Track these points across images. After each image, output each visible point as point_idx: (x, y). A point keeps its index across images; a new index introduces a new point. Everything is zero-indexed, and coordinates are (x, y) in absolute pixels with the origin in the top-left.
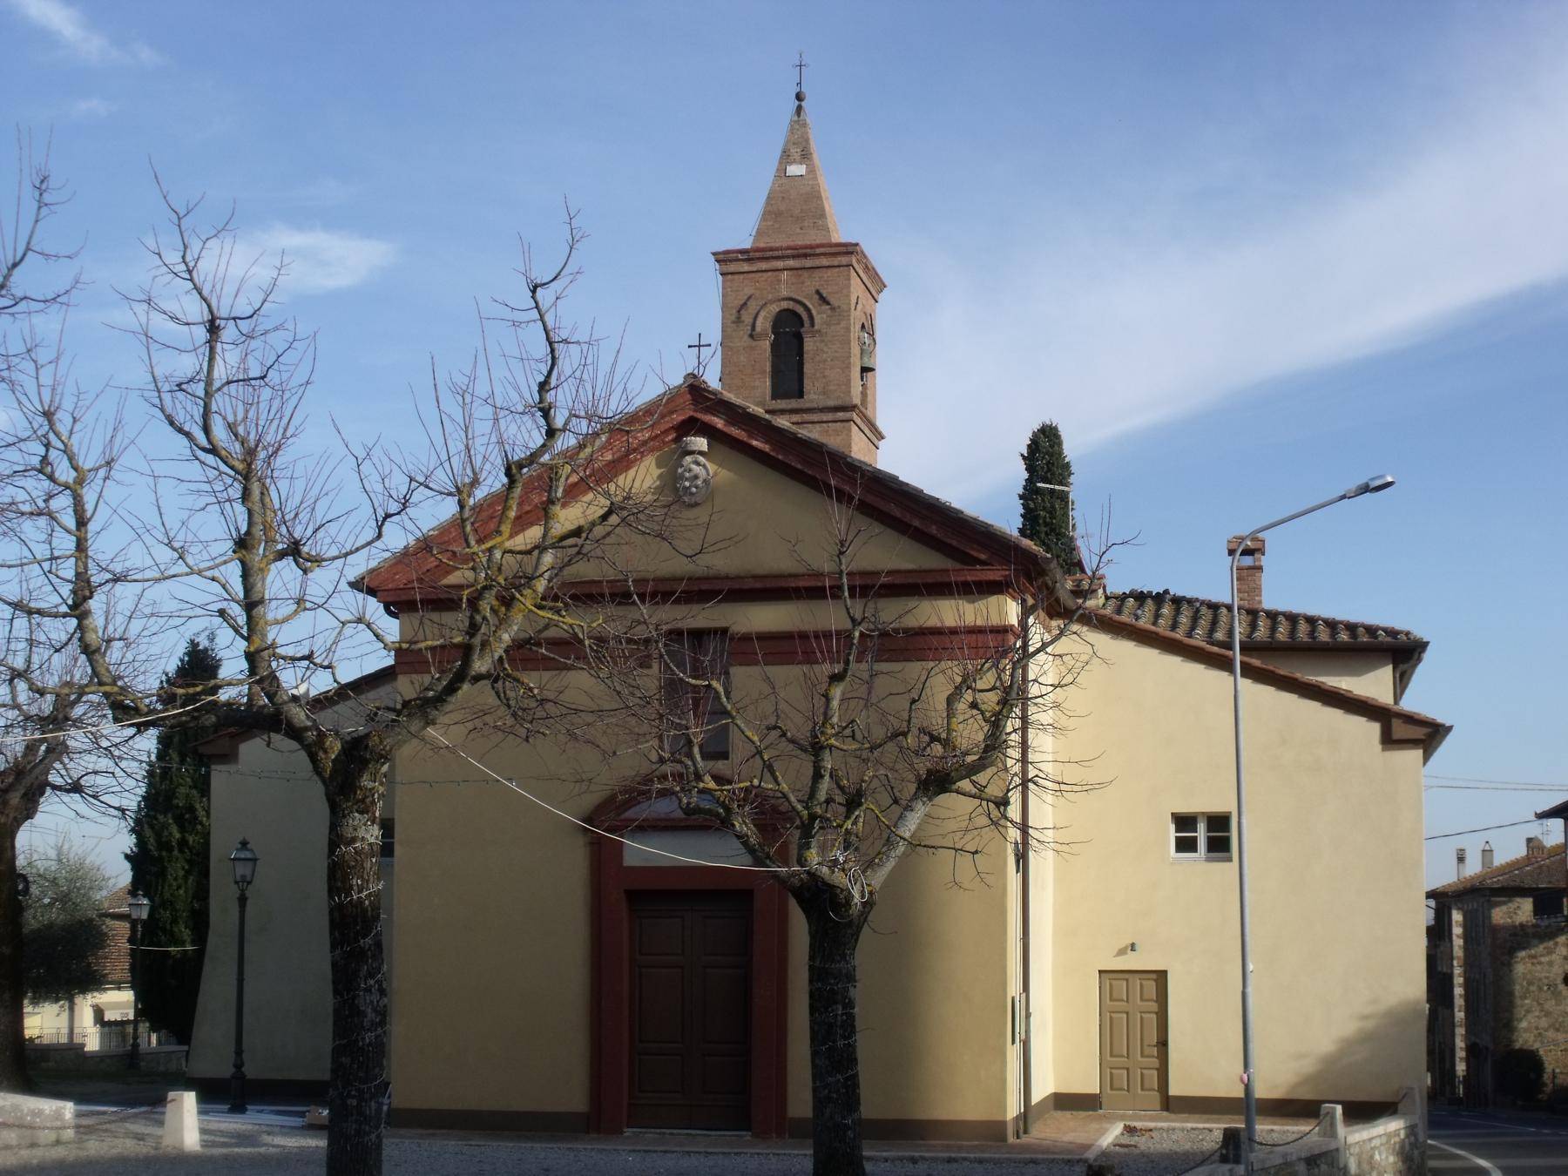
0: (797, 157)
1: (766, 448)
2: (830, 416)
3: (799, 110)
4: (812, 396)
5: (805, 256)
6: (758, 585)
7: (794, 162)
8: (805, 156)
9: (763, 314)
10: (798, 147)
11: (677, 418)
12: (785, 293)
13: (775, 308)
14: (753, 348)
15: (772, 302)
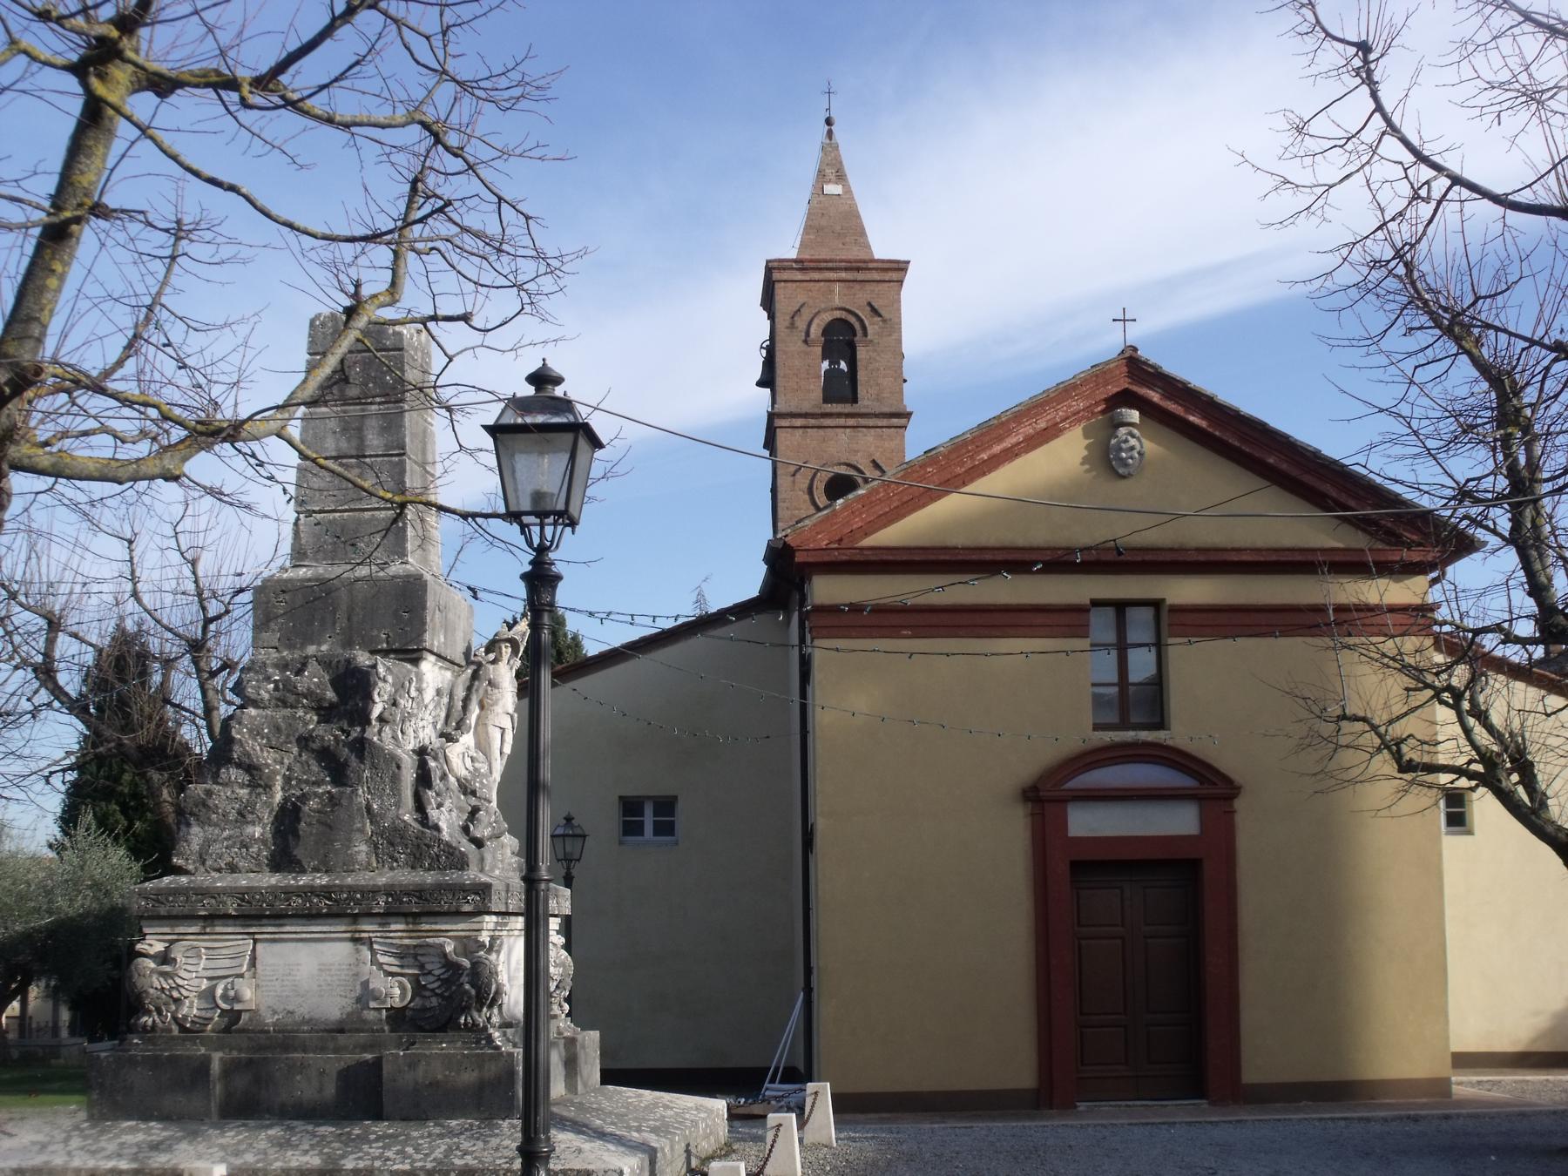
0: (833, 177)
1: (1203, 424)
2: (885, 422)
3: (830, 134)
4: (866, 403)
5: (858, 269)
6: (1202, 558)
7: (830, 181)
8: (841, 177)
9: (816, 321)
10: (832, 167)
11: (1113, 389)
12: (837, 302)
13: (827, 317)
14: (807, 354)
15: (825, 310)
